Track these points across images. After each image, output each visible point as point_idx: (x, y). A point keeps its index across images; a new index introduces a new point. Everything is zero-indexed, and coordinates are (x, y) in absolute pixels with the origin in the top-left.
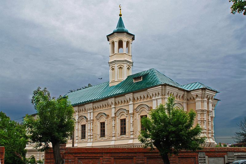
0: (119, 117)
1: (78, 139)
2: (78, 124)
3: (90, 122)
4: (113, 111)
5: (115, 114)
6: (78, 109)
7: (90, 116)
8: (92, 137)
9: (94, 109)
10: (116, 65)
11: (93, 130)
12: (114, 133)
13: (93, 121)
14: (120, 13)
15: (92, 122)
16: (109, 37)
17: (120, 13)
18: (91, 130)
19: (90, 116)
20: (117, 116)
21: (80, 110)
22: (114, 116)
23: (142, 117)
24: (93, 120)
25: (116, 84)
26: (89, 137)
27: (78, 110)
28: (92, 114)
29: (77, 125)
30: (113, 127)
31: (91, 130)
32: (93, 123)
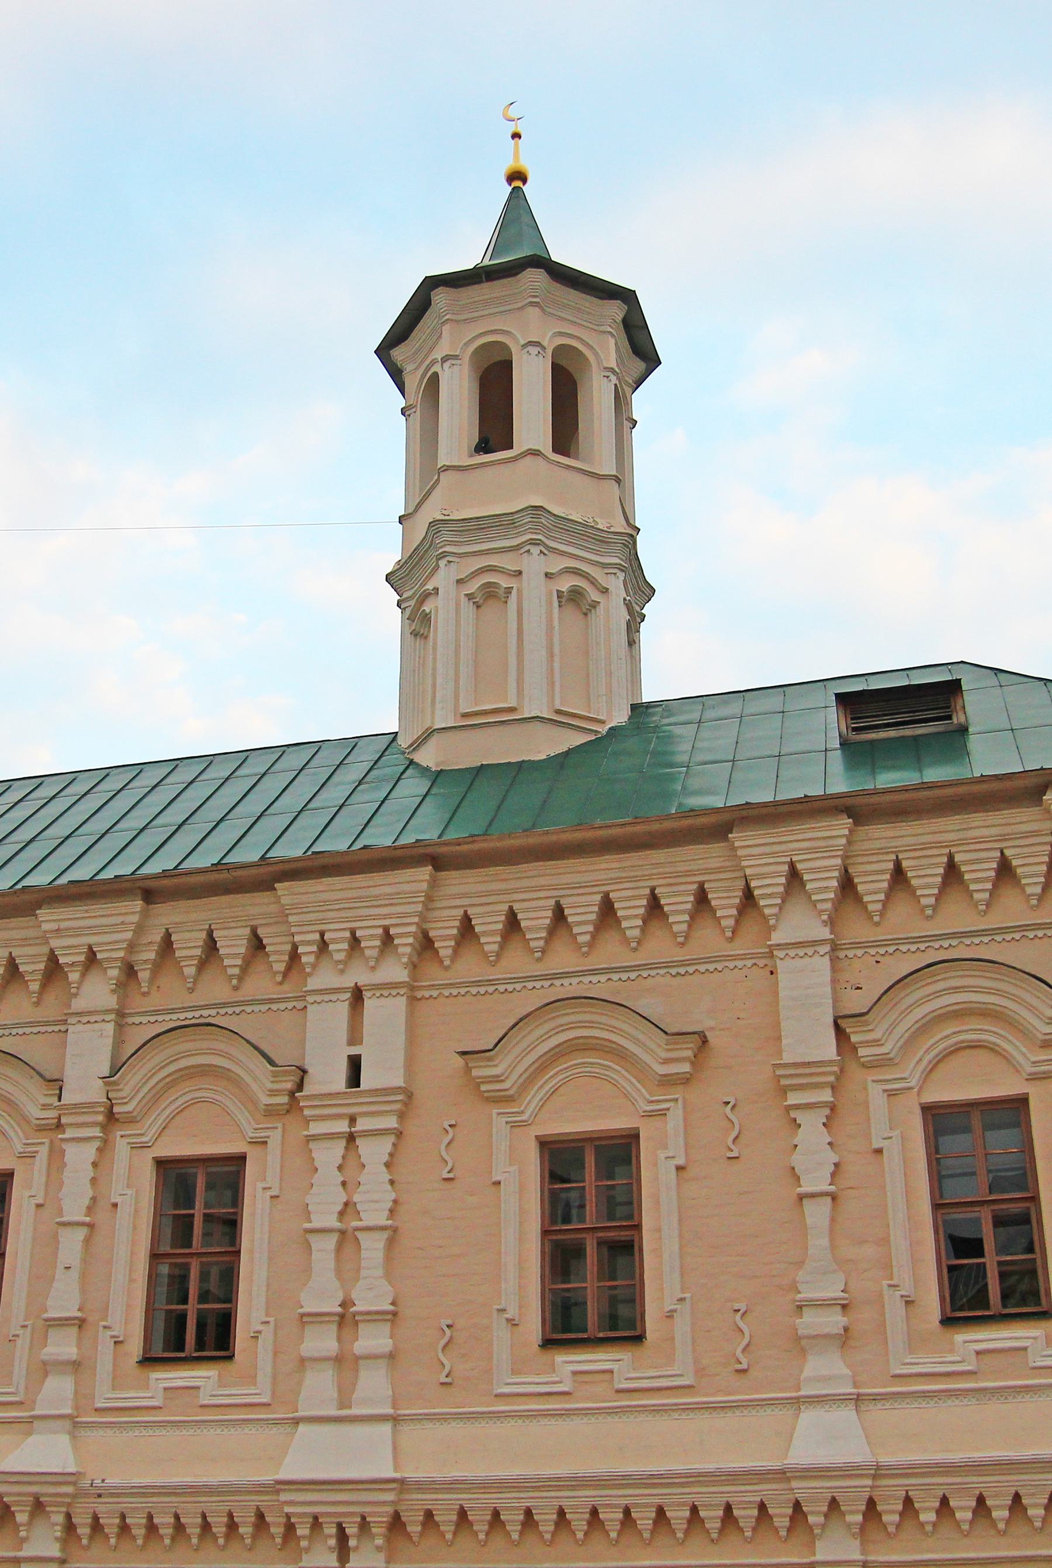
0: (911, 1072)
1: (75, 1366)
2: (105, 1147)
3: (343, 1126)
4: (806, 988)
5: (840, 1032)
6: (140, 929)
7: (355, 1036)
8: (373, 1339)
9: (426, 943)
10: (534, 564)
11: (393, 1235)
12: (834, 1291)
13: (402, 1116)
14: (516, 146)
15: (391, 1122)
16: (440, 297)
17: (516, 146)
18: (373, 1247)
19: (355, 1036)
20: (883, 1062)
21: (167, 945)
22: (827, 1048)
23: (941, 1120)
24: (406, 1099)
25: (546, 745)
26: (323, 1341)
27: (132, 947)
28: (385, 1015)
29: (90, 1151)
30: (817, 1213)
31: (373, 1247)
32: (399, 1134)
